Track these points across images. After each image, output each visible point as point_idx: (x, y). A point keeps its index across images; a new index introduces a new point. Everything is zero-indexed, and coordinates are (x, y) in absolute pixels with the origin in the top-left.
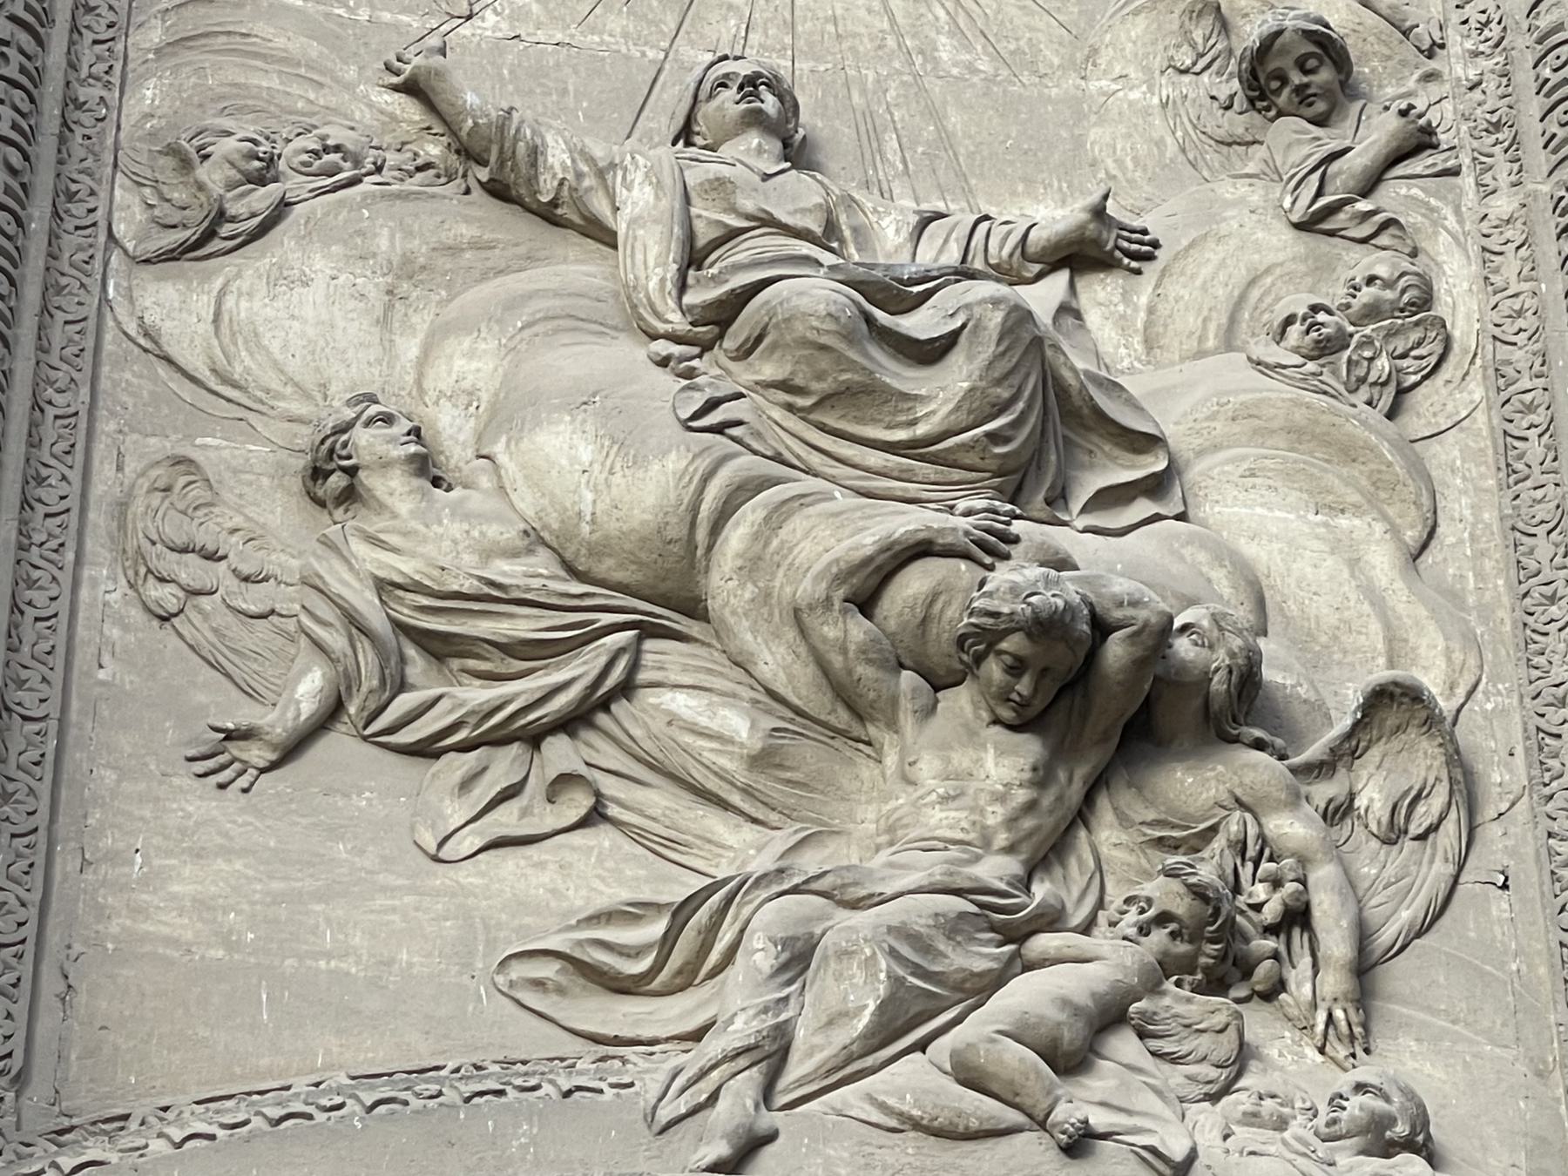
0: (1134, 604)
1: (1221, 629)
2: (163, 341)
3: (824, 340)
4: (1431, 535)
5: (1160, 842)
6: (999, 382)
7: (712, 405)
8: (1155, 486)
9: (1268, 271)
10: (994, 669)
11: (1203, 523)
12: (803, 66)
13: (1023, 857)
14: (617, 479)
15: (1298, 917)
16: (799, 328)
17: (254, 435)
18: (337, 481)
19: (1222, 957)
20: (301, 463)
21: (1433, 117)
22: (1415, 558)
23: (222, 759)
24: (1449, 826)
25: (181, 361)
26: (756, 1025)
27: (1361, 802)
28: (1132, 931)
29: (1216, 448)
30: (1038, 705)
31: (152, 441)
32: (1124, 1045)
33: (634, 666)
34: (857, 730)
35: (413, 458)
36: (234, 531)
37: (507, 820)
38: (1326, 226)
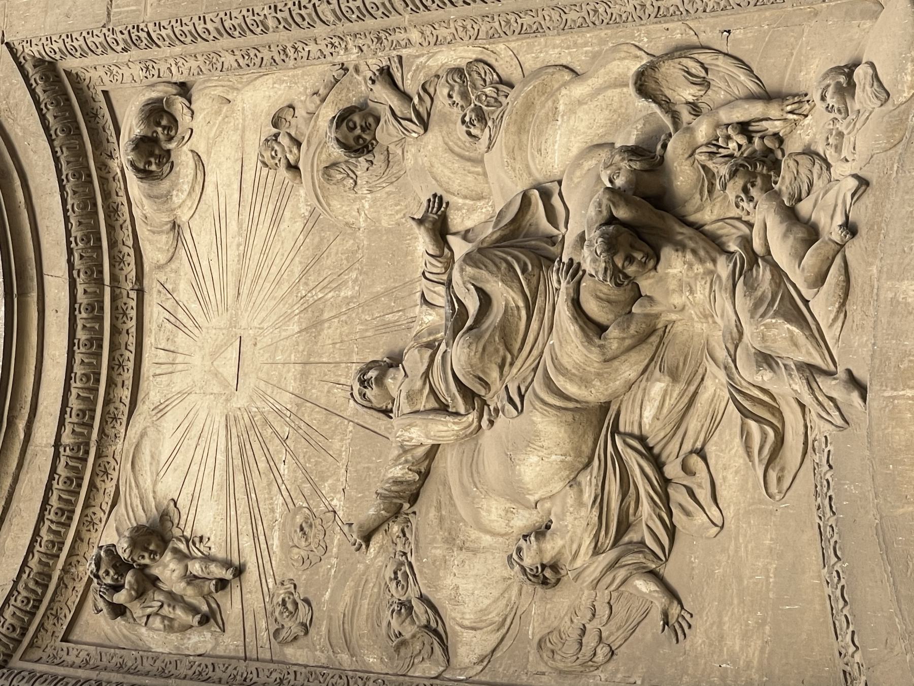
0: (600, 205)
1: (611, 165)
2: (485, 653)
3: (480, 349)
4: (566, 67)
5: (710, 192)
6: (499, 268)
7: (511, 401)
8: (546, 195)
9: (446, 144)
10: (631, 270)
11: (563, 172)
12: (355, 358)
13: (718, 256)
14: (545, 444)
15: (744, 128)
16: (475, 361)
17: (527, 612)
18: (548, 573)
19: (763, 163)
20: (540, 589)
21: (375, 68)
22: (577, 74)
23: (677, 626)
24: (701, 58)
25: (495, 645)
26: (797, 380)
27: (690, 99)
28: (752, 204)
29: (528, 166)
30: (647, 249)
31: (531, 659)
32: (804, 208)
33: (632, 436)
34: (660, 332)
35: (537, 539)
36: (572, 621)
37: (703, 494)
38: (425, 117)
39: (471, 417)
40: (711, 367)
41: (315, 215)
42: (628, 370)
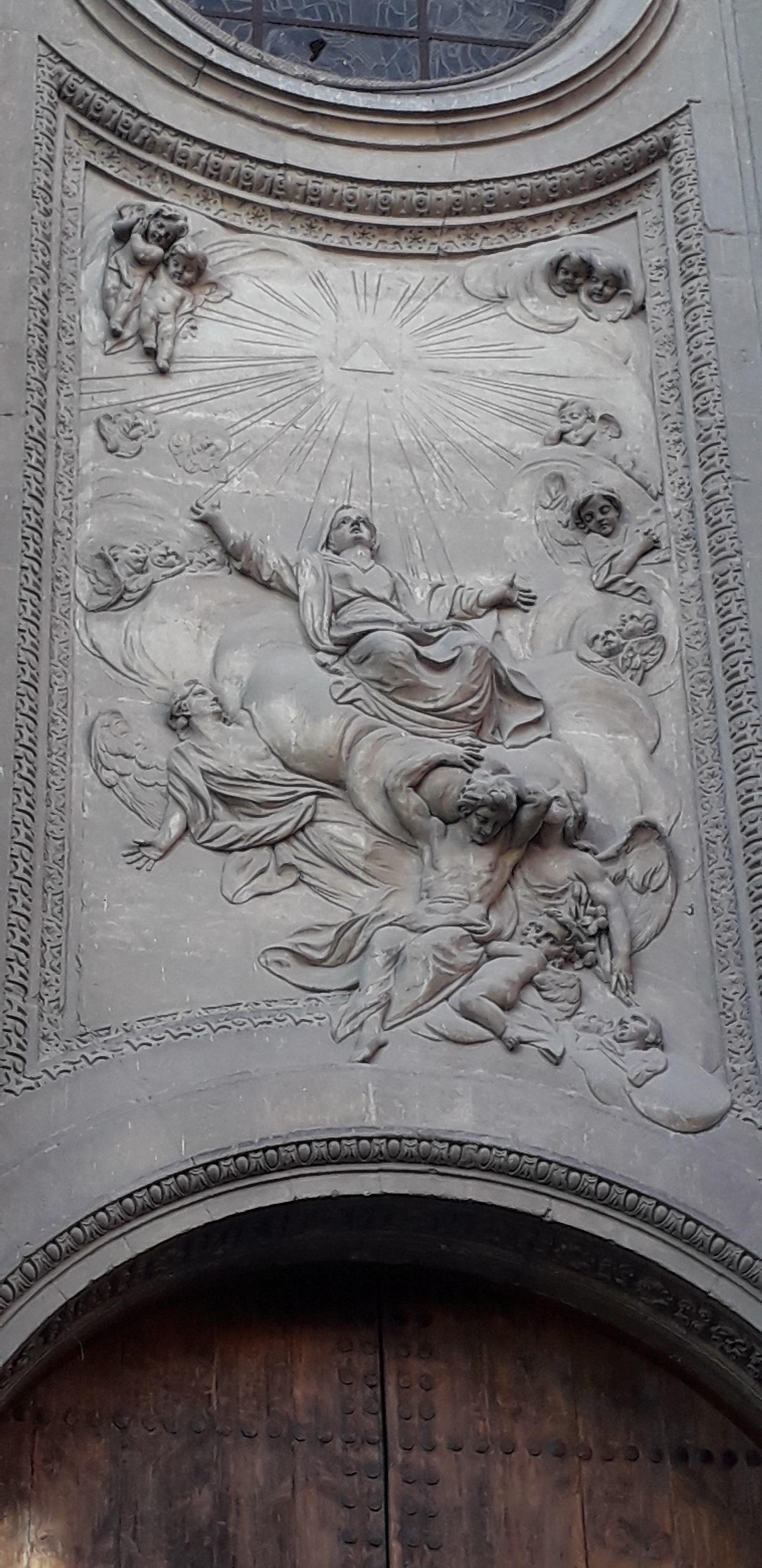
0: (536, 793)
3: (398, 664)
6: (474, 682)
10: (474, 822)
14: (307, 727)
18: (182, 721)
33: (315, 812)
35: (215, 713)
38: (610, 589)
39: (328, 641)
40: (382, 891)
41: (514, 460)
42: (377, 811)
